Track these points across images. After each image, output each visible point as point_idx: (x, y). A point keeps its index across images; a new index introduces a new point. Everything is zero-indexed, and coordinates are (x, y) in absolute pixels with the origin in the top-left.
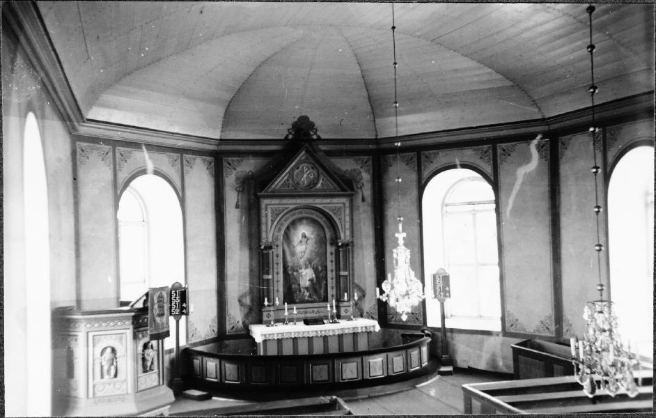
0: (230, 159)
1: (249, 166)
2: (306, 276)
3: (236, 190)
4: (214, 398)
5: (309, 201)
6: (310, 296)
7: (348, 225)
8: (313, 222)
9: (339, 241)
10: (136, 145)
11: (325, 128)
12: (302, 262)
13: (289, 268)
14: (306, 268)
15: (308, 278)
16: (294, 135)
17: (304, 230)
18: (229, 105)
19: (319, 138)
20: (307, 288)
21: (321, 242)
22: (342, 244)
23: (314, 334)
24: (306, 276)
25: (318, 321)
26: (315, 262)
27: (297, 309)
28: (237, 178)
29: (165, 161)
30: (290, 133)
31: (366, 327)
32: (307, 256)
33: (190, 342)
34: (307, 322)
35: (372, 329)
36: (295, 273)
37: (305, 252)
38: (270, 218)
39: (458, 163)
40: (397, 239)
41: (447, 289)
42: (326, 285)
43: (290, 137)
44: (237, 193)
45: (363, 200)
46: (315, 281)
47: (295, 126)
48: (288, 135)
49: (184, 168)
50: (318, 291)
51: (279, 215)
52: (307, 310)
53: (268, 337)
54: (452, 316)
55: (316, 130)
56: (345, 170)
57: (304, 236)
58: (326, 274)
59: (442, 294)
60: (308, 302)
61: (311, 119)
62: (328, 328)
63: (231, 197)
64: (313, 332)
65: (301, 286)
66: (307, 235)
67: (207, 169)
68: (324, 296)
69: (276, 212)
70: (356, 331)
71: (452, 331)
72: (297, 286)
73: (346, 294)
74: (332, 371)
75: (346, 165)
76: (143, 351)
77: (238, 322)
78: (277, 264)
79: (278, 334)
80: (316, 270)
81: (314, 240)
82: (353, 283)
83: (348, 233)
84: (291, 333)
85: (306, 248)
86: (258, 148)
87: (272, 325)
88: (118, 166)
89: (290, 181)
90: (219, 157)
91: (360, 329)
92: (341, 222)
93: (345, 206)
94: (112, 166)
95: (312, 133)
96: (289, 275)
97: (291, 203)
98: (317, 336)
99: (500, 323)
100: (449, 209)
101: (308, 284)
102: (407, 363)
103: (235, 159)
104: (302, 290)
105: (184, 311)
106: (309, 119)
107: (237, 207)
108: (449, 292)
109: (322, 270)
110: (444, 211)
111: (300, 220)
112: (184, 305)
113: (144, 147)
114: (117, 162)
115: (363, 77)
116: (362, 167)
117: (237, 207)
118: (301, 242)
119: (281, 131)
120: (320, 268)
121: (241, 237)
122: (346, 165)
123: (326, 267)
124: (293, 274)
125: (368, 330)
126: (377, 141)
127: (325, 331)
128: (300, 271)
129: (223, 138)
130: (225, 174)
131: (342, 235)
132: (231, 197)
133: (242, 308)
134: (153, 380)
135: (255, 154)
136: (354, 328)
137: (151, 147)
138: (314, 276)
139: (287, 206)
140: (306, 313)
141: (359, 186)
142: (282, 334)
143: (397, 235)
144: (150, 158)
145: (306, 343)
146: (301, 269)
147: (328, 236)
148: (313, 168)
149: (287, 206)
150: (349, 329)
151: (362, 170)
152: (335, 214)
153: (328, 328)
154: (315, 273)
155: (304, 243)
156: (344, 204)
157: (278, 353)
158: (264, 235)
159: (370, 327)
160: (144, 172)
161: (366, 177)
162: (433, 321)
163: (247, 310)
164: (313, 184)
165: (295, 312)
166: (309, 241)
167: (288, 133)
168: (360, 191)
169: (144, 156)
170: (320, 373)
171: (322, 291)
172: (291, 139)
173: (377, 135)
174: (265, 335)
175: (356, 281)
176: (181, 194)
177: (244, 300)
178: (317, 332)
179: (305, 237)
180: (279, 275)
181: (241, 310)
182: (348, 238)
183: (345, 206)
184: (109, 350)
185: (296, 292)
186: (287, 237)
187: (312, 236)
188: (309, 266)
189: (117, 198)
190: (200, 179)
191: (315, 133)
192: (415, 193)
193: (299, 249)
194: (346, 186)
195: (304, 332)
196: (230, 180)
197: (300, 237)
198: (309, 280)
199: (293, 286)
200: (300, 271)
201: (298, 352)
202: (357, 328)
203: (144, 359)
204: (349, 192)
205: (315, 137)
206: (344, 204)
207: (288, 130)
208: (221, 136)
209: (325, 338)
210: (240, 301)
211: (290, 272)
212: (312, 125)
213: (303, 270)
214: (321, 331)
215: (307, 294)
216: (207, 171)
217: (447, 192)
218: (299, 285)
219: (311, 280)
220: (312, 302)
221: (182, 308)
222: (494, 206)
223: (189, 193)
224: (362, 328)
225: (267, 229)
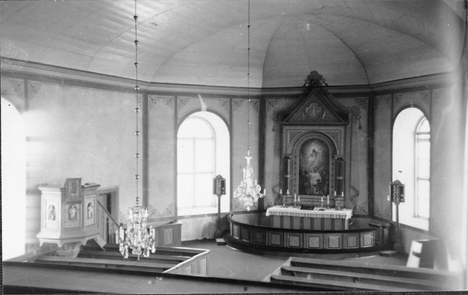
0: (270, 100)
1: (281, 104)
2: (315, 177)
3: (273, 120)
4: (227, 246)
5: (316, 128)
6: (317, 191)
7: (342, 146)
8: (321, 142)
9: (335, 156)
10: (195, 95)
11: (330, 77)
12: (312, 168)
13: (303, 172)
14: (315, 172)
15: (316, 179)
16: (309, 84)
17: (314, 147)
18: (264, 67)
19: (327, 86)
20: (315, 186)
21: (326, 156)
22: (338, 158)
23: (303, 216)
24: (315, 177)
25: (311, 208)
26: (322, 168)
27: (300, 198)
29: (216, 103)
30: (307, 83)
31: (340, 216)
32: (315, 164)
33: (233, 211)
34: (303, 207)
36: (307, 175)
37: (314, 162)
38: (289, 139)
39: (412, 103)
40: (246, 160)
41: (402, 195)
42: (328, 185)
43: (307, 85)
44: (273, 122)
45: (360, 128)
46: (321, 182)
47: (309, 77)
48: (305, 84)
49: (233, 107)
50: (323, 188)
51: (294, 136)
52: (314, 200)
53: (273, 214)
54: (418, 216)
55: (324, 80)
56: (347, 106)
57: (314, 151)
58: (329, 177)
59: (398, 199)
60: (315, 195)
61: (319, 73)
62: (316, 212)
63: (270, 125)
64: (302, 214)
65: (311, 184)
66: (316, 150)
67: (253, 106)
69: (294, 135)
70: (333, 217)
71: (404, 226)
72: (308, 184)
73: (343, 193)
74: (282, 239)
75: (348, 103)
76: (69, 209)
77: (271, 203)
78: (295, 168)
79: (280, 213)
80: (322, 174)
81: (321, 154)
83: (342, 151)
84: (287, 213)
85: (315, 160)
86: (286, 93)
87: (284, 207)
88: (178, 107)
89: (303, 115)
90: (262, 100)
91: (335, 216)
92: (338, 144)
93: (341, 132)
94: (174, 107)
95: (321, 82)
97: (305, 129)
98: (305, 217)
99: (427, 222)
100: (421, 137)
101: (315, 183)
102: (359, 242)
103: (274, 100)
104: (312, 186)
105: (223, 192)
106: (317, 73)
108: (403, 198)
109: (326, 175)
110: (416, 138)
111: (312, 140)
112: (223, 189)
113: (200, 96)
114: (178, 104)
115: (345, 43)
116: (360, 105)
117: (273, 130)
118: (312, 155)
119: (300, 81)
120: (324, 173)
121: (275, 150)
122: (348, 103)
123: (329, 173)
124: (305, 175)
126: (369, 86)
127: (311, 214)
129: (265, 87)
130: (266, 109)
131: (338, 153)
132: (270, 125)
133: (274, 194)
134: (76, 224)
135: (286, 96)
136: (331, 215)
137: (204, 95)
138: (320, 178)
140: (313, 201)
141: (358, 118)
142: (282, 213)
143: (246, 158)
144: (204, 102)
145: (320, 220)
146: (311, 172)
147: (331, 152)
148: (319, 106)
150: (327, 215)
151: (360, 107)
152: (333, 137)
153: (316, 212)
154: (321, 175)
155: (314, 156)
156: (341, 131)
157: (322, 228)
158: (284, 149)
159: (342, 216)
160: (199, 110)
161: (363, 113)
162: (394, 219)
164: (320, 116)
165: (299, 200)
166: (318, 155)
167: (305, 82)
168: (358, 121)
169: (200, 102)
170: (275, 240)
171: (325, 189)
172: (308, 87)
173: (369, 82)
174: (271, 212)
175: (352, 184)
176: (229, 122)
177: (275, 190)
178: (305, 214)
179: (315, 152)
180: (296, 176)
181: (273, 195)
182: (342, 154)
183: (341, 132)
184: (51, 207)
185: (307, 188)
186: (302, 151)
189: (176, 126)
190: (247, 114)
191: (324, 82)
192: (390, 124)
193: (311, 159)
194: (343, 117)
195: (296, 213)
196: (270, 113)
197: (312, 152)
200: (311, 174)
201: (313, 228)
202: (333, 215)
203: (70, 214)
205: (324, 85)
207: (305, 80)
208: (263, 86)
209: (312, 219)
210: (273, 190)
211: (304, 174)
212: (321, 77)
214: (308, 214)
215: (315, 189)
216: (253, 108)
217: (418, 124)
218: (310, 183)
219: (318, 181)
221: (222, 190)
222: (428, 136)
223: (235, 122)
224: (337, 215)
225: (286, 145)
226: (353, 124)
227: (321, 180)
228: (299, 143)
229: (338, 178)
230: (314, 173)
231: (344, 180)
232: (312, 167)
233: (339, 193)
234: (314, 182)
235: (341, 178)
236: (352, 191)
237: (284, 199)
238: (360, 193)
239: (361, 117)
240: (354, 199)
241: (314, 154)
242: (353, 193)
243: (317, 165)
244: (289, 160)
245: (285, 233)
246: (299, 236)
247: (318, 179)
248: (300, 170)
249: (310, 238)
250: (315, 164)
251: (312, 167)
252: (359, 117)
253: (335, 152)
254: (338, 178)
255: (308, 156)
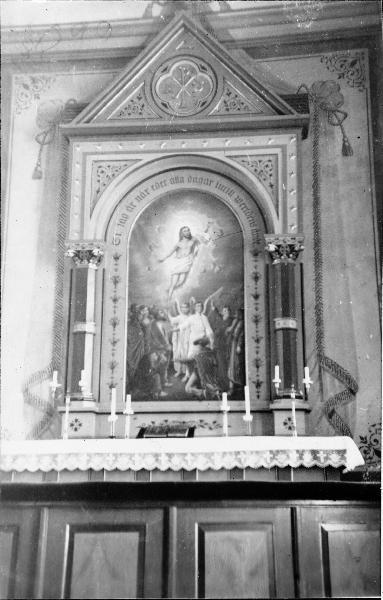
6: (197, 384)
8: (211, 202)
9: (268, 238)
12: (177, 297)
13: (146, 311)
14: (191, 311)
20: (190, 364)
21: (233, 249)
24: (189, 333)
28: (40, 117)
32: (193, 282)
35: (335, 461)
36: (160, 325)
37: (187, 273)
42: (242, 355)
45: (346, 151)
46: (211, 346)
50: (219, 373)
58: (242, 328)
60: (193, 397)
68: (235, 386)
72: (164, 358)
80: (214, 319)
81: (211, 245)
82: (320, 357)
96: (144, 328)
104: (177, 367)
107: (37, 176)
109: (231, 319)
111: (177, 196)
117: (37, 176)
118: (177, 249)
120: (225, 313)
121: (40, 242)
124: (154, 325)
125: (323, 463)
128: (173, 320)
131: (277, 225)
133: (30, 409)
138: (209, 332)
139: (138, 156)
149: (138, 156)
151: (342, 82)
156: (283, 148)
163: (40, 415)
168: (337, 129)
171: (231, 373)
175: (329, 353)
179: (190, 237)
181: (25, 413)
182: (293, 230)
185: (160, 371)
186: (141, 238)
187: (207, 236)
188: (198, 307)
198: (196, 343)
199: (154, 357)
200: (173, 320)
204: (296, 115)
206: (283, 148)
211: (147, 321)
213: (181, 317)
218: (170, 354)
219: (202, 343)
220: (201, 399)
226: (321, 141)
227: (212, 341)
228: (131, 207)
229: (281, 323)
230: (187, 313)
231: (300, 330)
232: (180, 292)
233: (291, 377)
234: (185, 348)
235: (291, 323)
236: (327, 378)
237: (67, 419)
238: (362, 385)
239: (346, 115)
240: (340, 410)
241: (186, 244)
242: (333, 387)
243: (196, 284)
244: (92, 266)
245: (46, 513)
246: (140, 528)
247: (200, 336)
248: (132, 308)
249: (208, 535)
250: (188, 280)
251: (180, 292)
252: (341, 116)
253: (267, 228)
254: (281, 323)
255: (162, 254)
